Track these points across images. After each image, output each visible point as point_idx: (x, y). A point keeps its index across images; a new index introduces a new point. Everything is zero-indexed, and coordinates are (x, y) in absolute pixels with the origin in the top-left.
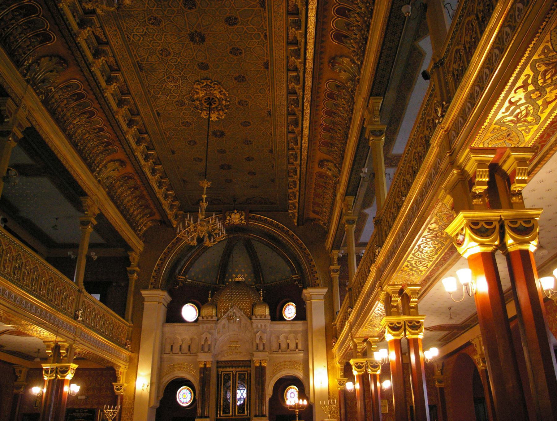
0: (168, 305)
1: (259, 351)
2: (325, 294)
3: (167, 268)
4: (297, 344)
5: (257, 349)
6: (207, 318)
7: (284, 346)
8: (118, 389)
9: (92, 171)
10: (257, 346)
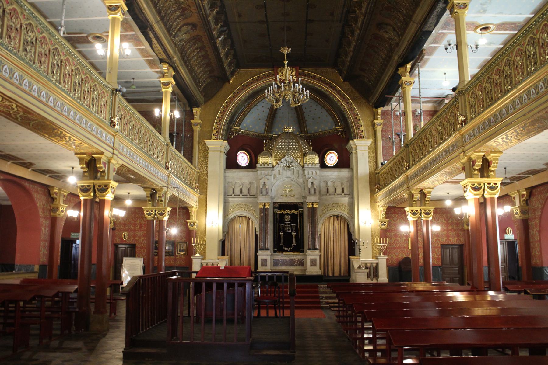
0: (227, 152)
1: (311, 195)
3: (226, 120)
4: (343, 189)
5: (309, 193)
7: (331, 190)
8: (191, 225)
9: (170, 35)
10: (309, 191)
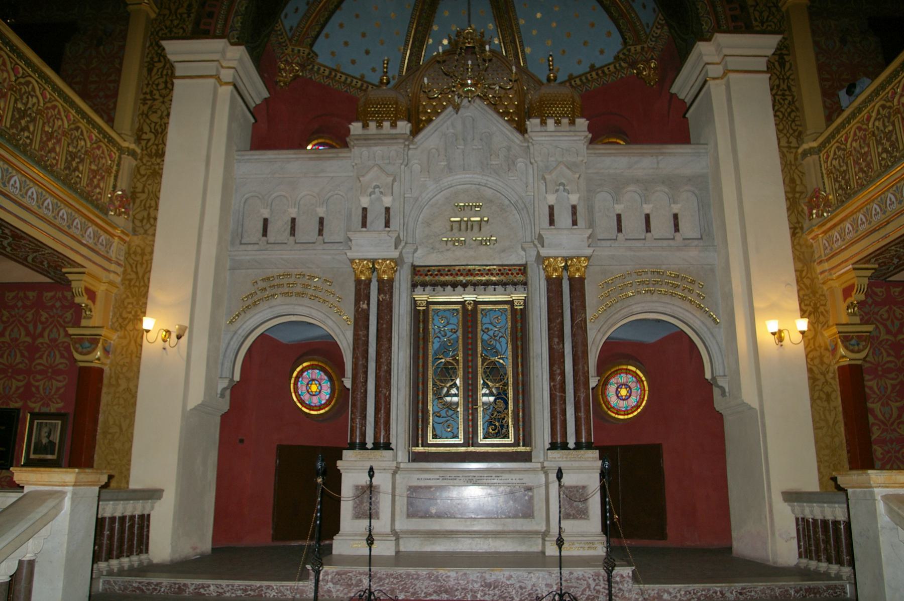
2: (770, 52)
6: (380, 126)
